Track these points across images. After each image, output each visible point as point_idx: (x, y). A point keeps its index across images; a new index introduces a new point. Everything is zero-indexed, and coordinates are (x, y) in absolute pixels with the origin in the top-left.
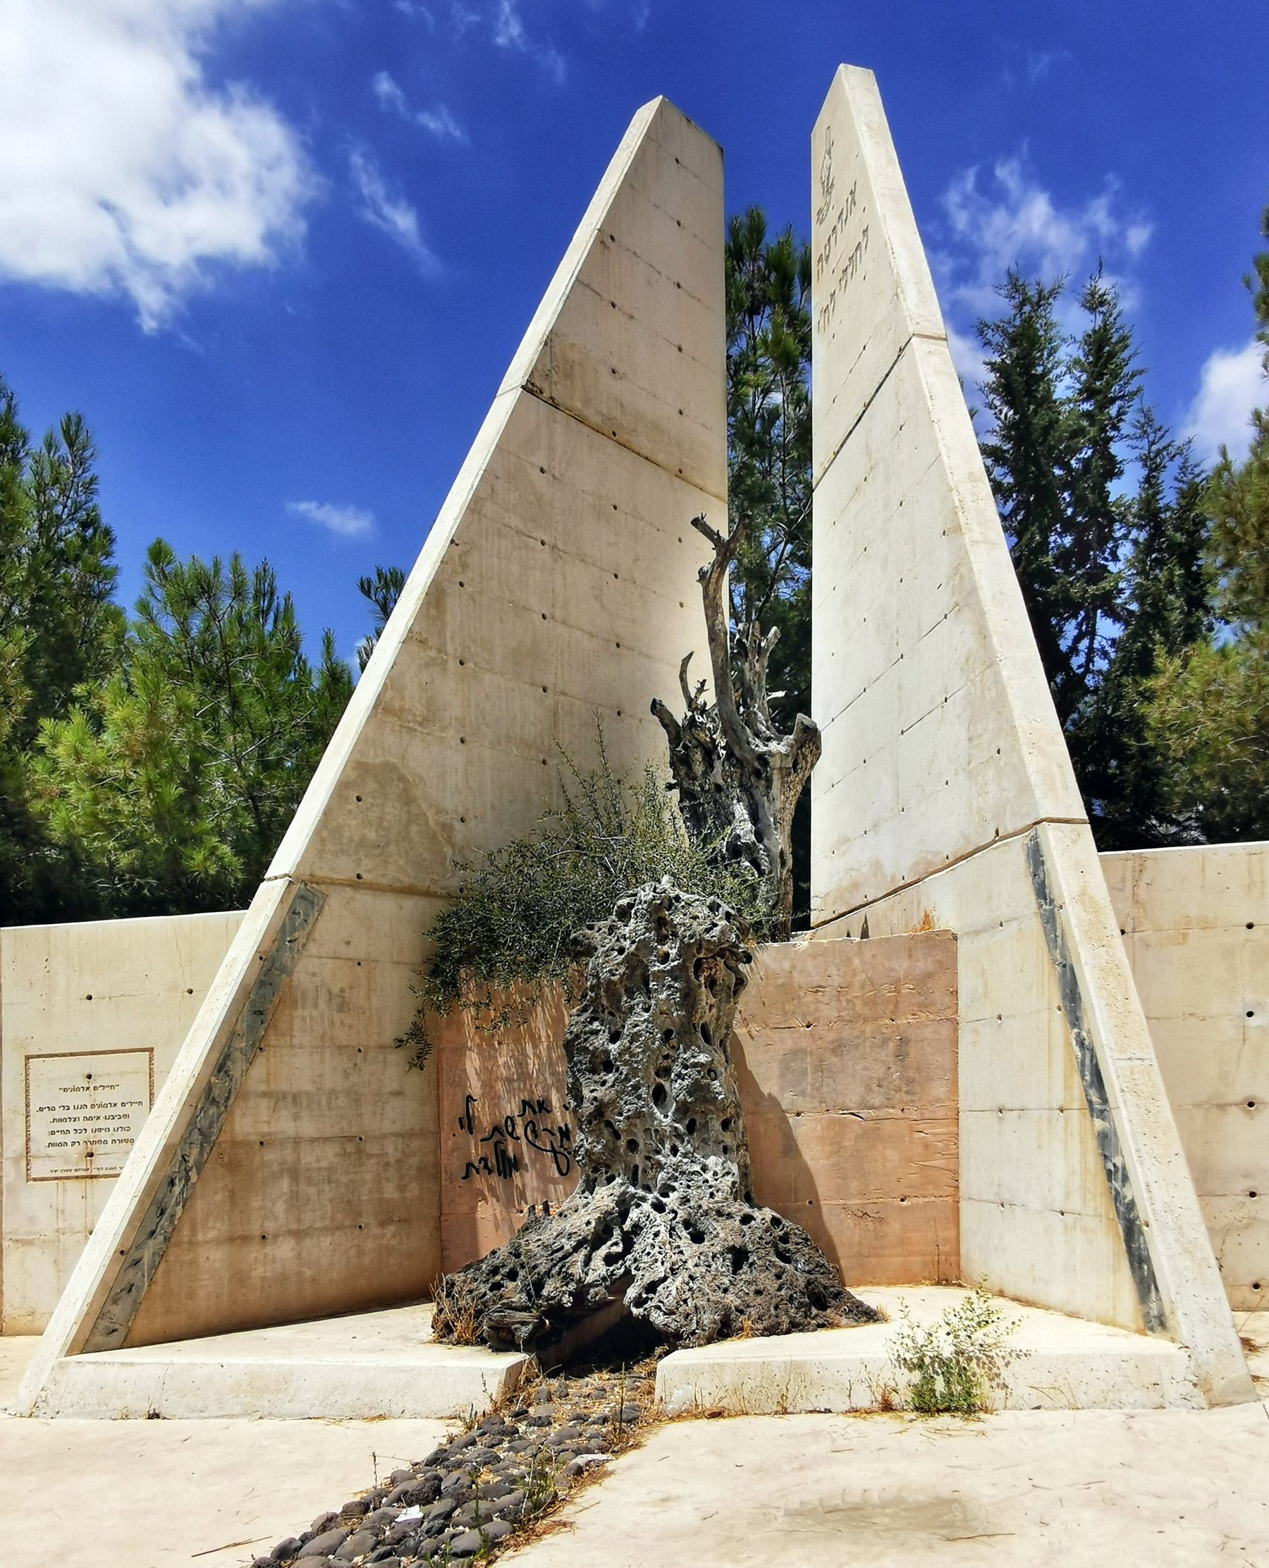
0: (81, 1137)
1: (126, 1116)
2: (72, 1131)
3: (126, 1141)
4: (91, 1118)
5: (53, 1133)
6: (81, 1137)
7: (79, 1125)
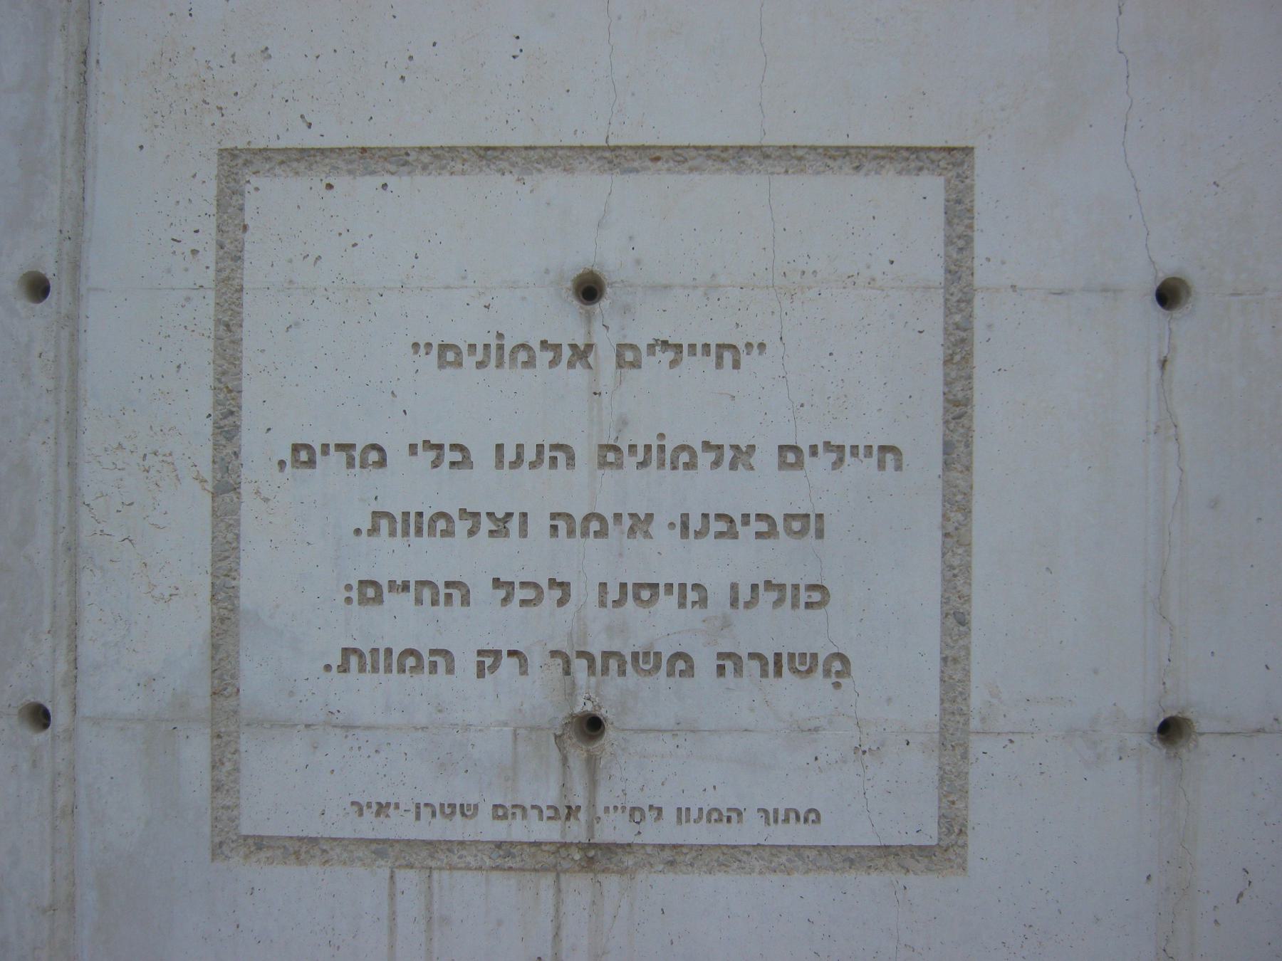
0: (539, 628)
1: (806, 524)
2: (482, 590)
3: (805, 665)
4: (595, 525)
5: (370, 592)
6: (539, 628)
7: (530, 557)
